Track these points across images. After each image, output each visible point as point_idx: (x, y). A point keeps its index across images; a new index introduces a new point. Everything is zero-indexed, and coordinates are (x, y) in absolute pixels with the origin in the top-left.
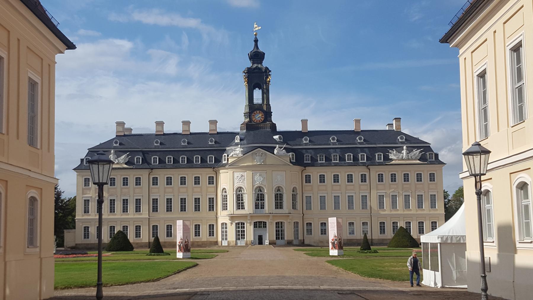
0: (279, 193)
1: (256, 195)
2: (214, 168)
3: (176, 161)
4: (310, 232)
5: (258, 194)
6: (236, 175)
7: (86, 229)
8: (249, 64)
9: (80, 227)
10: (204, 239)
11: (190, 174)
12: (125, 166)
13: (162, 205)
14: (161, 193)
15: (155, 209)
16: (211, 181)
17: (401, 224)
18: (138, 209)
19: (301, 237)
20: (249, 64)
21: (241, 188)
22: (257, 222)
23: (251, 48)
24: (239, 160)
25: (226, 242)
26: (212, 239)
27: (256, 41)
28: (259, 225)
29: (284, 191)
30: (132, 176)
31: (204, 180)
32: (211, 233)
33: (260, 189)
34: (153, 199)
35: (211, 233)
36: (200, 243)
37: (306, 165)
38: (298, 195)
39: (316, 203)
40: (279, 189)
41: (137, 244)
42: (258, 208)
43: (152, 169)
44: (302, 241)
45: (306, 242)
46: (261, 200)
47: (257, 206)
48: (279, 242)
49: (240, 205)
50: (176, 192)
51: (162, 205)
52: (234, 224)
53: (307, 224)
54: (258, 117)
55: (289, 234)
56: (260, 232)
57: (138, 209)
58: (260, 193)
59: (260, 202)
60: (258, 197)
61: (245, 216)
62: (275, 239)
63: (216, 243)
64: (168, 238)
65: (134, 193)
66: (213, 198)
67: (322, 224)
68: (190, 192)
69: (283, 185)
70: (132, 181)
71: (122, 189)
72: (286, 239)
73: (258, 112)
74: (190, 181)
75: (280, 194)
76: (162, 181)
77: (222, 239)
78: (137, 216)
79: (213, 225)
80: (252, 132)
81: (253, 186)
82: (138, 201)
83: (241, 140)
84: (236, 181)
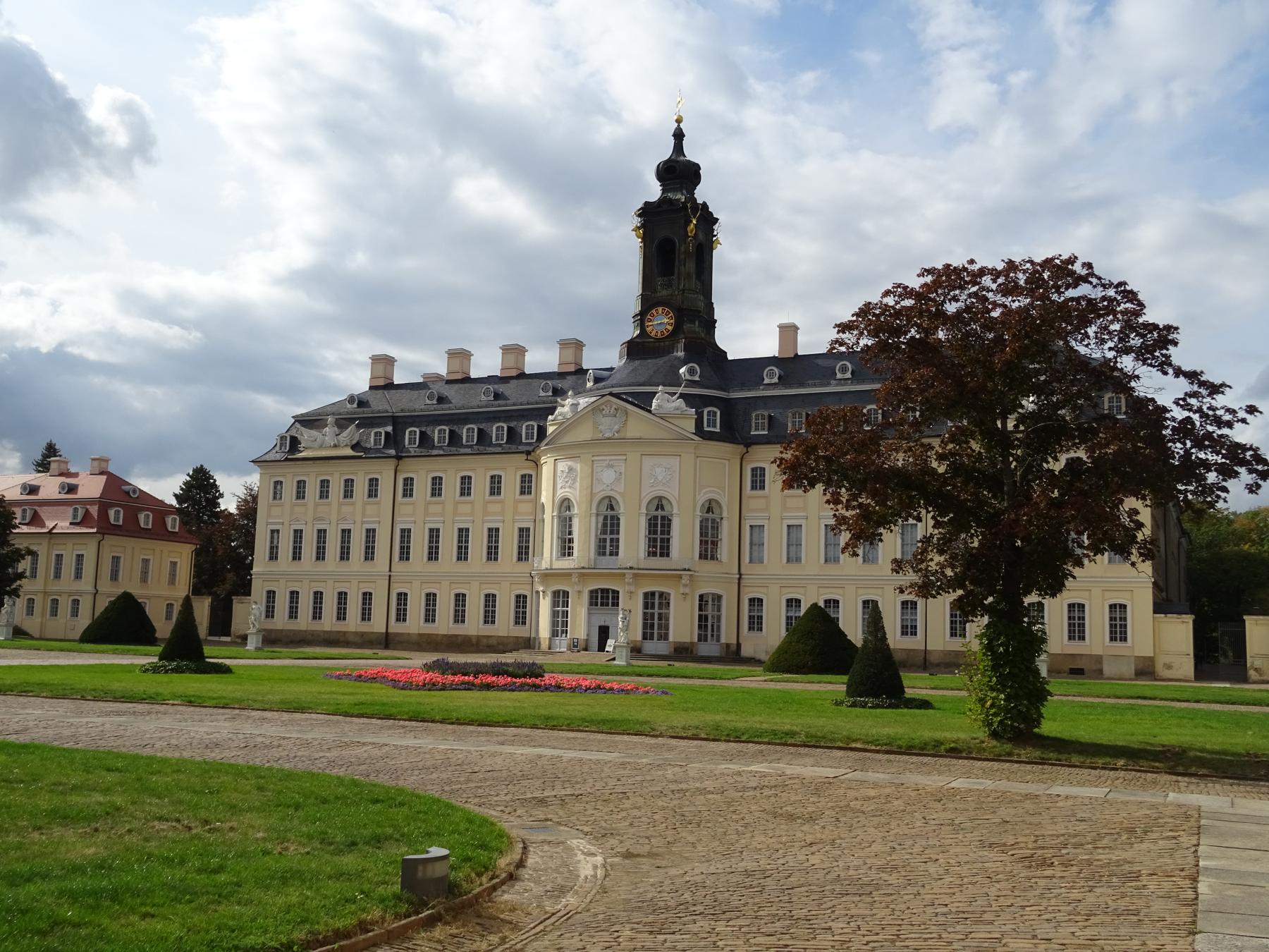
0: (660, 513)
1: (601, 519)
2: (528, 453)
3: (454, 439)
5: (606, 518)
7: (271, 595)
8: (654, 191)
10: (503, 633)
11: (481, 470)
12: (350, 452)
13: (419, 545)
14: (419, 514)
15: (405, 554)
16: (527, 485)
17: (810, 597)
18: (369, 554)
20: (654, 191)
22: (596, 591)
23: (666, 152)
26: (521, 631)
27: (679, 136)
28: (604, 599)
29: (675, 511)
30: (361, 474)
31: (511, 483)
32: (520, 618)
34: (403, 531)
35: (520, 618)
36: (493, 642)
37: (749, 442)
38: (725, 524)
39: (775, 543)
41: (363, 634)
42: (604, 554)
44: (734, 648)
45: (746, 651)
46: (612, 533)
47: (601, 551)
48: (651, 647)
50: (450, 513)
51: (419, 545)
53: (752, 601)
55: (682, 625)
56: (602, 618)
57: (369, 554)
58: (610, 513)
59: (608, 537)
60: (605, 525)
61: (565, 575)
62: (639, 637)
63: (529, 644)
64: (456, 626)
65: (364, 515)
66: (528, 530)
67: (789, 601)
68: (478, 513)
69: (672, 493)
70: (361, 488)
71: (340, 505)
72: (671, 639)
73: (660, 309)
74: (481, 485)
75: (663, 518)
76: (422, 486)
79: (525, 597)
80: (637, 363)
81: (592, 495)
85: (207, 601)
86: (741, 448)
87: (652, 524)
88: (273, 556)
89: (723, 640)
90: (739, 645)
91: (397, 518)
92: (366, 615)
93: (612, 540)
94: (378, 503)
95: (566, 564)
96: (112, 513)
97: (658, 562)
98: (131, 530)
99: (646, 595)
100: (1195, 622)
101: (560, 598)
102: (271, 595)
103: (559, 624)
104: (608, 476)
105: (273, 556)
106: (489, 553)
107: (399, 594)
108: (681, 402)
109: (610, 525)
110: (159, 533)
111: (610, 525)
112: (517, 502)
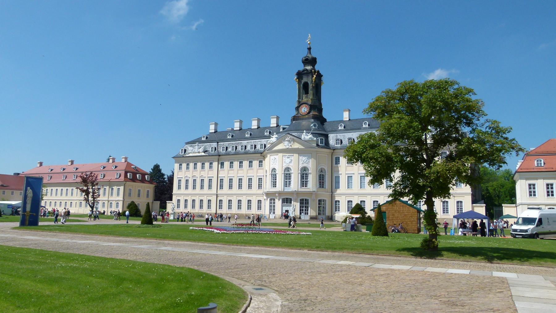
2: (261, 153)
4: (337, 209)
6: (272, 157)
7: (179, 201)
9: (175, 198)
12: (203, 154)
13: (226, 184)
15: (221, 187)
18: (210, 187)
19: (328, 213)
21: (275, 169)
23: (304, 54)
24: (274, 145)
25: (274, 215)
28: (287, 201)
33: (288, 169)
35: (259, 208)
38: (327, 176)
40: (305, 169)
43: (219, 156)
49: (274, 185)
51: (226, 184)
52: (269, 199)
54: (304, 109)
57: (210, 187)
59: (288, 180)
61: (274, 193)
62: (299, 214)
75: (306, 174)
77: (270, 213)
78: (210, 192)
82: (210, 181)
83: (284, 129)
84: (271, 163)
85: (159, 202)
86: (332, 151)
87: (302, 177)
88: (179, 187)
89: (327, 214)
90: (332, 216)
91: (219, 176)
92: (209, 207)
93: (289, 182)
94: (213, 170)
95: (274, 190)
96: (128, 174)
97: (304, 189)
98: (134, 179)
99: (301, 200)
100: (486, 207)
101: (272, 201)
102: (179, 201)
103: (272, 209)
104: (288, 160)
105: (179, 187)
106: (249, 186)
107: (220, 200)
108: (310, 136)
109: (287, 176)
110: (143, 181)
111: (287, 176)
112: (257, 170)
